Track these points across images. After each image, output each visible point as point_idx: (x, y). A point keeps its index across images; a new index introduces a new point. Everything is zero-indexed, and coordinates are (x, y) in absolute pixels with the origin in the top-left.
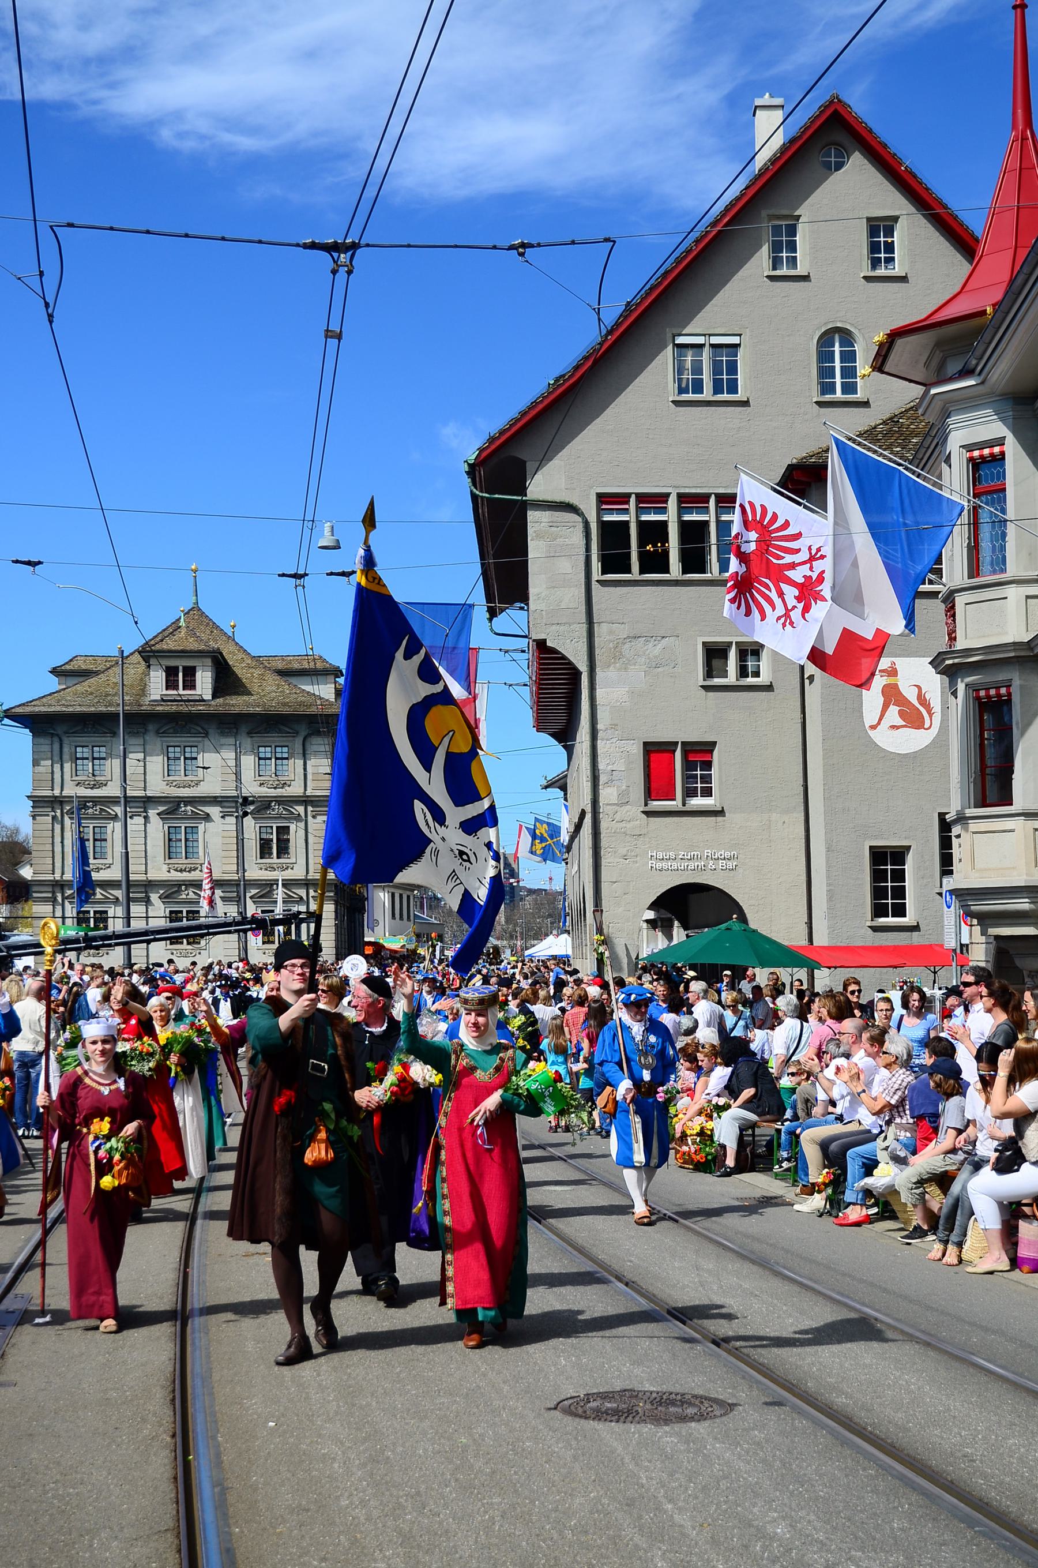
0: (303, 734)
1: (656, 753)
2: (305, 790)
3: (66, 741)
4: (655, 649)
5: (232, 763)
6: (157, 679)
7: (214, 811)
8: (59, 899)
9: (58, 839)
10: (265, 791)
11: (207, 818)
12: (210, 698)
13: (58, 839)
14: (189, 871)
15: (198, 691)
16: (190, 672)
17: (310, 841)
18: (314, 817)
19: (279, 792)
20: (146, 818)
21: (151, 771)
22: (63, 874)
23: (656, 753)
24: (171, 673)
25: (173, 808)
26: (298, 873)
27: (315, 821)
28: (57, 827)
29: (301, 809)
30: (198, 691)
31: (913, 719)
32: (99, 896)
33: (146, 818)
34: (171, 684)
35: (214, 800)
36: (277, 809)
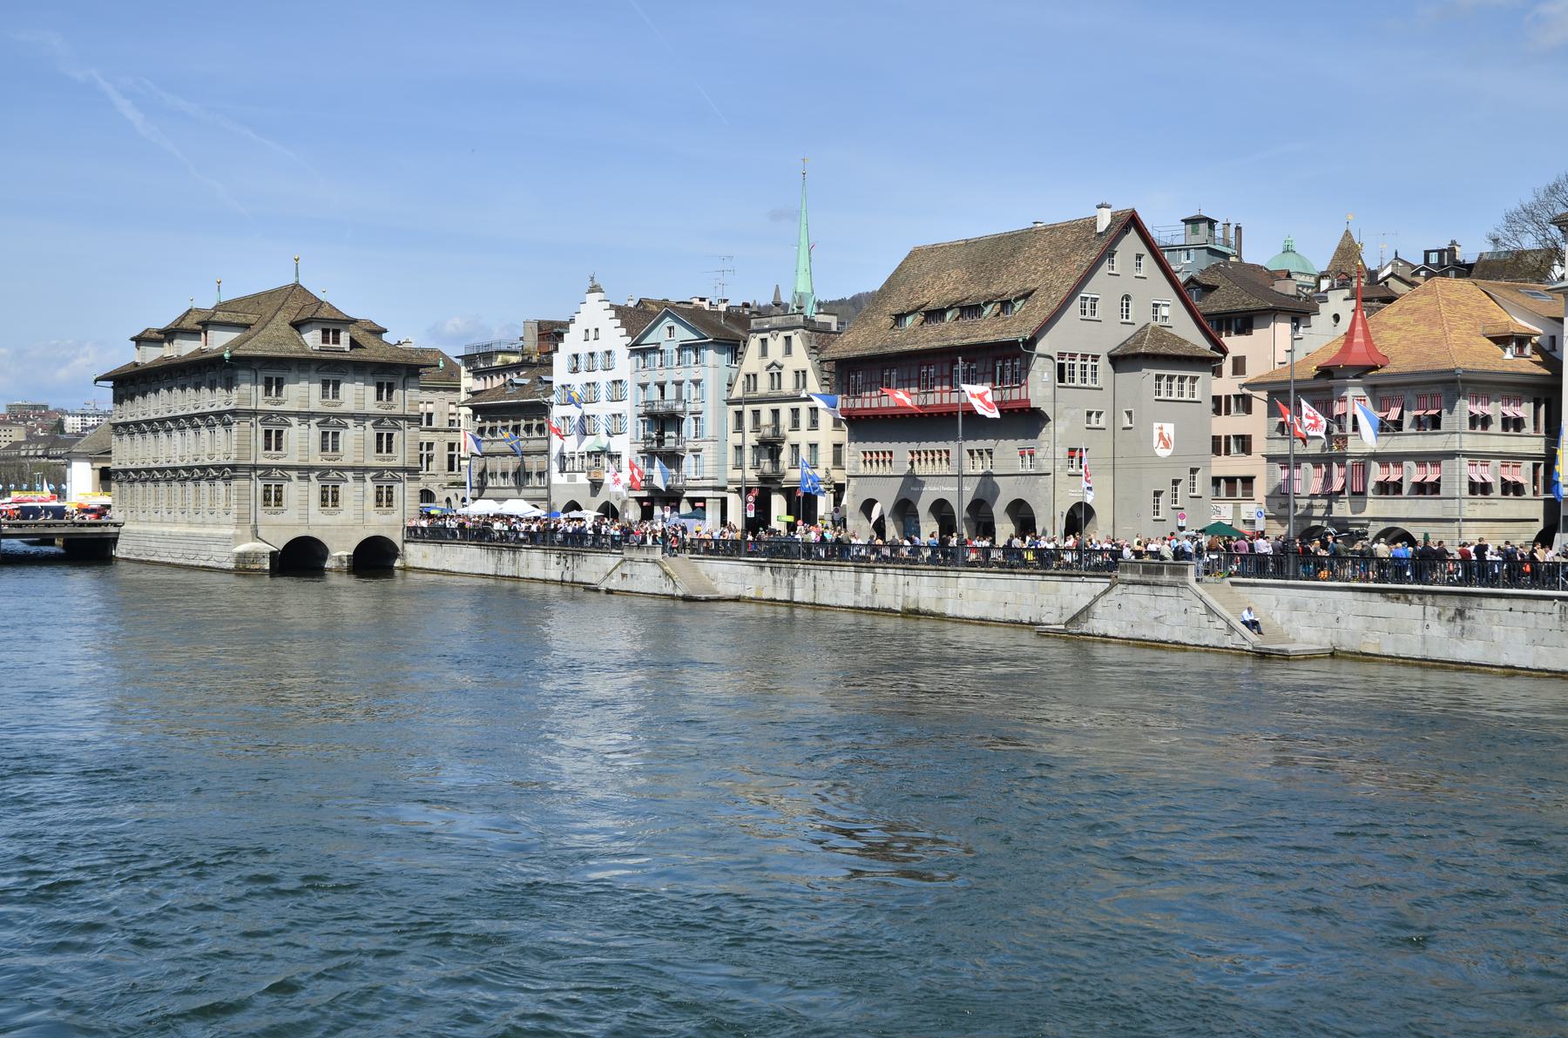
1: (1072, 450)
4: (1072, 412)
7: (350, 422)
10: (381, 411)
11: (346, 427)
12: (347, 349)
16: (336, 333)
21: (302, 393)
23: (1072, 450)
24: (325, 332)
25: (325, 419)
26: (398, 463)
31: (1167, 446)
34: (325, 340)
35: (352, 416)
36: (387, 423)
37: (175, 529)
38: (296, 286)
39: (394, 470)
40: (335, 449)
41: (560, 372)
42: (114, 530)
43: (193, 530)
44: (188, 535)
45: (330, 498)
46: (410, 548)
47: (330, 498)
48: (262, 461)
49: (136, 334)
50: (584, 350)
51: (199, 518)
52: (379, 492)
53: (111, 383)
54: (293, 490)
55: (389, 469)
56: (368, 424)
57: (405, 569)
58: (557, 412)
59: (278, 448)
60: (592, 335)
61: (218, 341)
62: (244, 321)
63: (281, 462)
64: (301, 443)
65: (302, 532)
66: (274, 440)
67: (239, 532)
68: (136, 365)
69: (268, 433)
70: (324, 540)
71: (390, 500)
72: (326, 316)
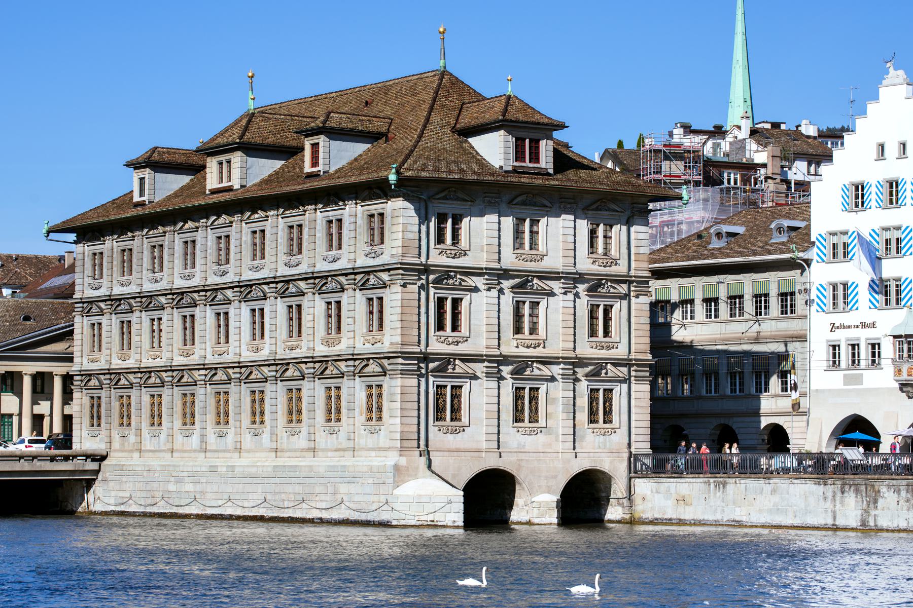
0: (628, 213)
2: (629, 270)
3: (430, 205)
5: (571, 239)
6: (494, 149)
7: (556, 286)
8: (423, 371)
9: (423, 310)
10: (596, 269)
11: (551, 294)
12: (551, 171)
13: (423, 310)
14: (535, 348)
15: (542, 164)
17: (633, 320)
18: (637, 297)
19: (608, 270)
20: (501, 291)
22: (427, 346)
26: (620, 352)
27: (638, 300)
28: (423, 294)
29: (623, 289)
30: (542, 164)
32: (458, 370)
33: (501, 291)
37: (242, 462)
38: (443, 73)
39: (617, 363)
40: (533, 330)
41: (826, 211)
42: (91, 466)
43: (284, 461)
44: (276, 470)
45: (525, 408)
46: (642, 486)
47: (525, 408)
48: (436, 347)
49: (139, 152)
50: (875, 175)
51: (301, 442)
52: (593, 400)
53: (72, 237)
54: (482, 397)
55: (608, 360)
56: (582, 288)
57: (632, 522)
58: (822, 273)
59: (455, 328)
60: (892, 150)
61: (336, 157)
62: (369, 127)
63: (462, 349)
64: (484, 316)
65: (491, 462)
66: (448, 315)
67: (403, 461)
68: (141, 204)
69: (441, 302)
70: (519, 476)
71: (608, 413)
72: (521, 117)
